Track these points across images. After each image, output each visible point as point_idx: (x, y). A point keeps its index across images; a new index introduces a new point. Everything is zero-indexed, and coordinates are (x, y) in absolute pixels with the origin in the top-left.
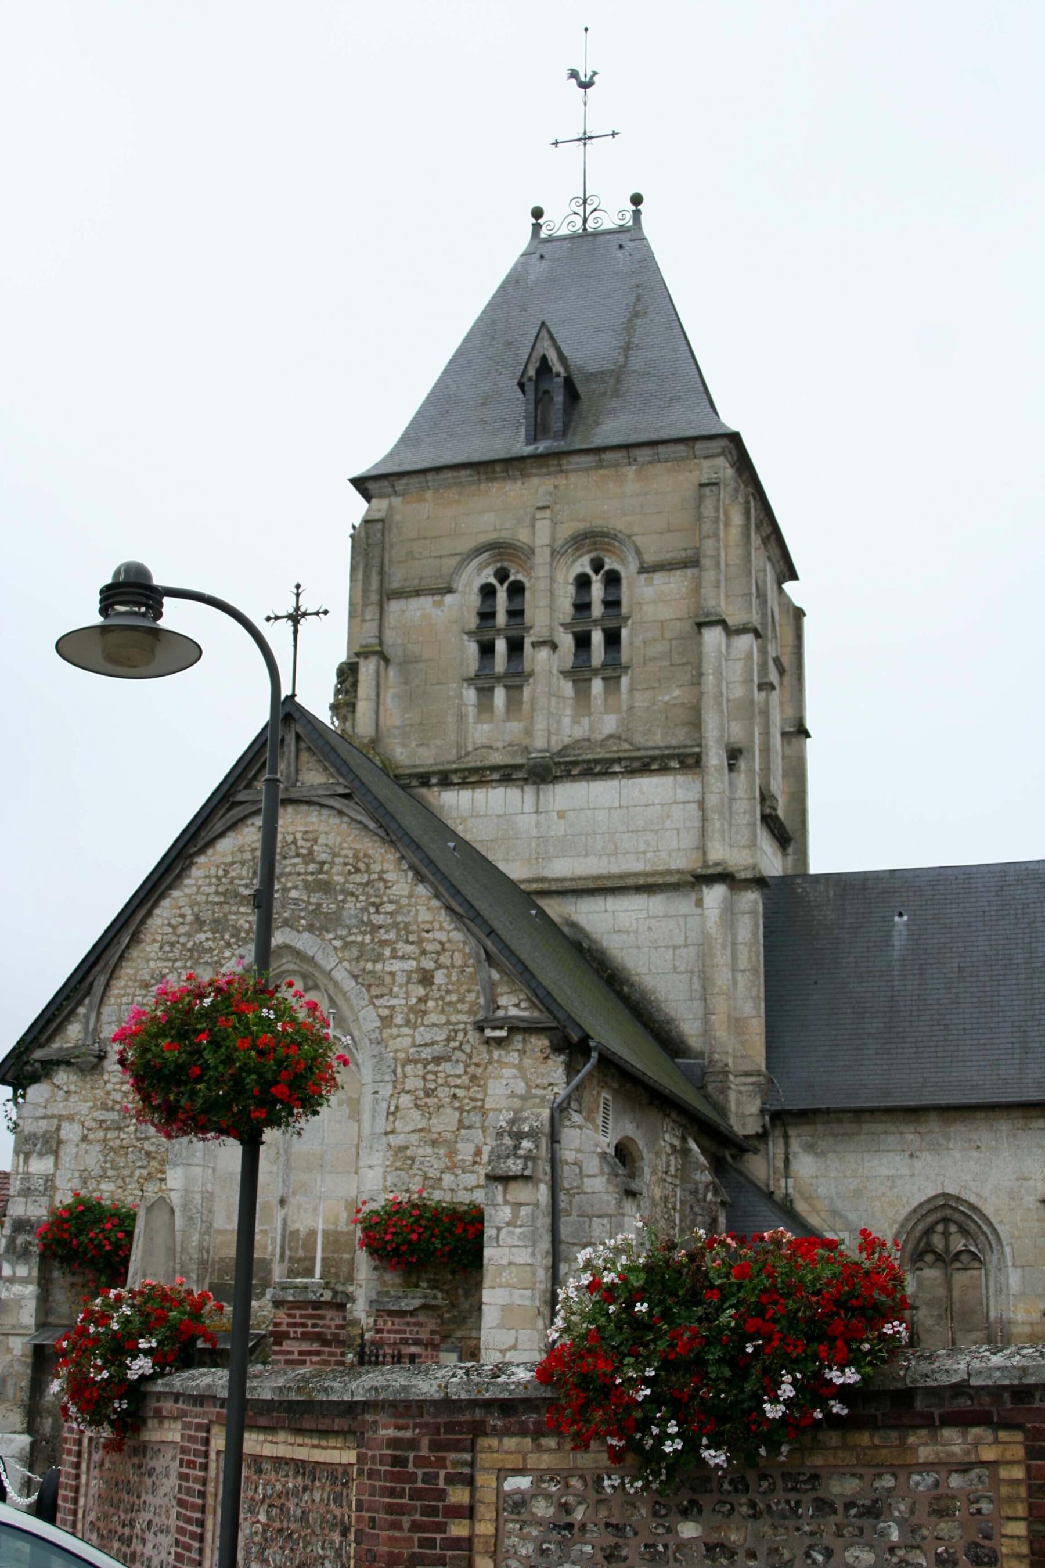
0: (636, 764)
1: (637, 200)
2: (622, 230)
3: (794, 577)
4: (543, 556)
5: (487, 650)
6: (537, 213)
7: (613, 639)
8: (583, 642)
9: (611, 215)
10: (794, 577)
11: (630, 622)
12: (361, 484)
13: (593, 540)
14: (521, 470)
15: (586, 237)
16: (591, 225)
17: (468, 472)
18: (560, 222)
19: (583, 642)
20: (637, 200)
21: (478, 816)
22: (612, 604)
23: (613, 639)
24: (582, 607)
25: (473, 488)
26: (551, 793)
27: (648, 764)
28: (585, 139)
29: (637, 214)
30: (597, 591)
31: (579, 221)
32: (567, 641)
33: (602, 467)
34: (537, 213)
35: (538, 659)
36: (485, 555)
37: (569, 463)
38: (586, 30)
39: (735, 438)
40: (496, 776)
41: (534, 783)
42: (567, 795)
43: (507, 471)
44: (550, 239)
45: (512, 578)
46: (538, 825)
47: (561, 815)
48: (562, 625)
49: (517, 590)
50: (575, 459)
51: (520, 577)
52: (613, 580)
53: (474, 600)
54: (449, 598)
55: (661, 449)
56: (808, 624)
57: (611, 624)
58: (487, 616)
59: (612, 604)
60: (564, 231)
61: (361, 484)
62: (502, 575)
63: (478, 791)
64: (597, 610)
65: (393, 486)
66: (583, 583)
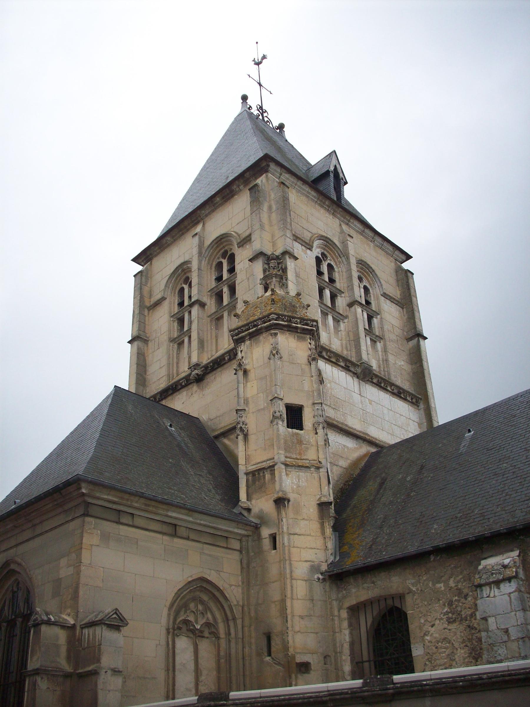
0: (395, 391)
6: (245, 98)
11: (378, 317)
14: (335, 211)
17: (315, 194)
21: (335, 383)
25: (313, 204)
26: (364, 387)
27: (400, 393)
33: (362, 235)
34: (245, 98)
37: (353, 223)
38: (257, 43)
40: (342, 364)
41: (358, 377)
42: (372, 392)
43: (329, 207)
45: (329, 262)
46: (362, 402)
47: (371, 402)
50: (356, 223)
51: (332, 263)
54: (308, 251)
55: (385, 244)
63: (334, 368)
65: (281, 174)
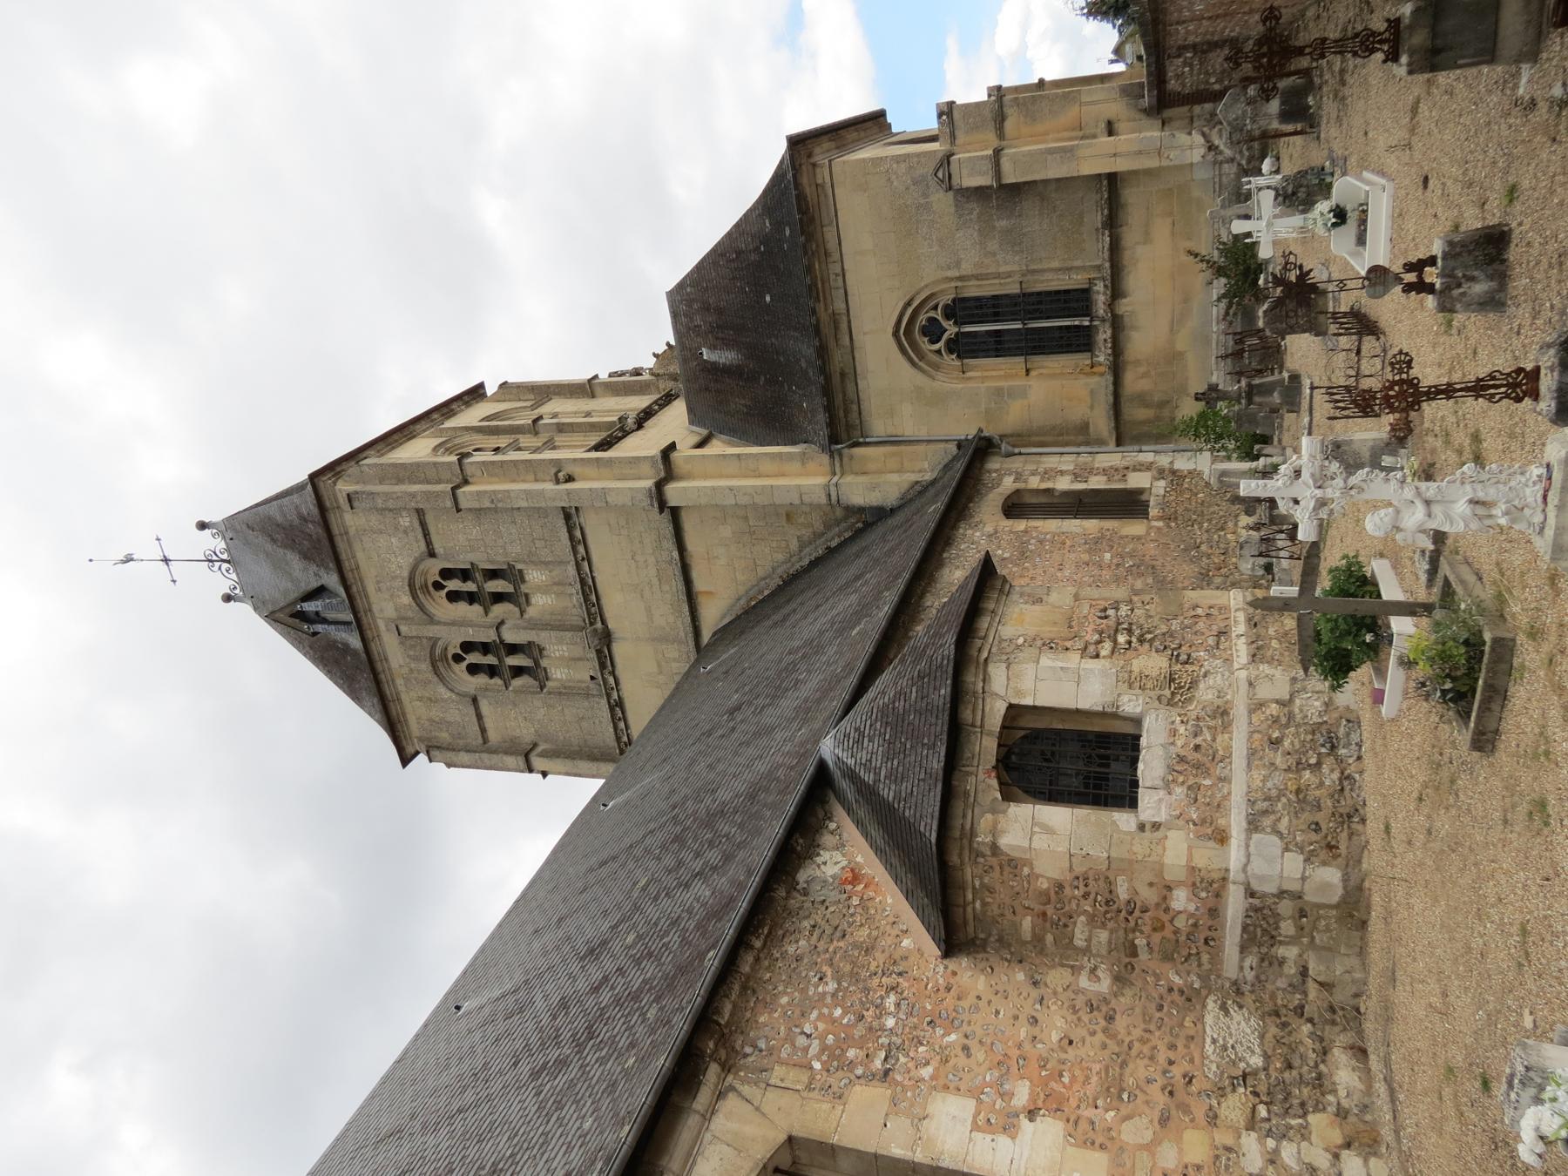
1: (202, 526)
3: (481, 386)
4: (433, 631)
7: (493, 574)
8: (498, 598)
10: (481, 386)
12: (405, 761)
16: (225, 557)
20: (202, 526)
22: (465, 575)
23: (493, 574)
24: (471, 598)
30: (454, 585)
31: (225, 566)
32: (499, 610)
34: (228, 598)
35: (510, 637)
36: (442, 670)
39: (314, 477)
48: (486, 613)
49: (468, 647)
52: (447, 574)
53: (482, 680)
56: (513, 379)
57: (478, 576)
59: (465, 575)
60: (234, 576)
61: (405, 761)
62: (458, 659)
66: (453, 597)
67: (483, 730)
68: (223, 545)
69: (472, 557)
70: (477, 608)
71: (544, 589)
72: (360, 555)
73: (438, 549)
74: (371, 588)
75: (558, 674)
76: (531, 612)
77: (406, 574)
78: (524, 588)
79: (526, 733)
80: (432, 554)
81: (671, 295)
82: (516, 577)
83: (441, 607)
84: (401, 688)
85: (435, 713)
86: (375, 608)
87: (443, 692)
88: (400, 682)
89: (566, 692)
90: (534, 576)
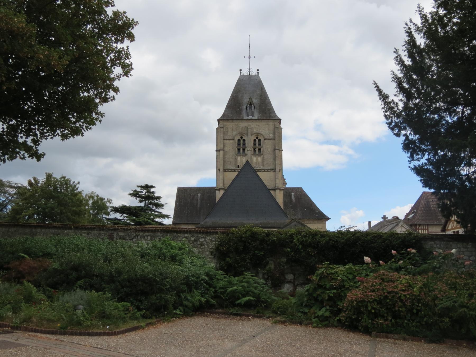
1: (258, 70)
2: (256, 76)
5: (239, 150)
6: (241, 70)
7: (260, 150)
9: (254, 73)
13: (258, 134)
15: (250, 76)
18: (245, 73)
19: (255, 150)
20: (258, 70)
22: (260, 144)
23: (260, 150)
24: (255, 144)
28: (250, 57)
29: (258, 73)
32: (253, 149)
34: (241, 70)
44: (243, 76)
52: (260, 140)
57: (260, 147)
58: (239, 144)
59: (260, 144)
64: (257, 145)
66: (255, 140)
67: (226, 140)
68: (253, 74)
69: (264, 147)
70: (253, 145)
71: (257, 160)
72: (264, 123)
73: (266, 141)
74: (257, 123)
75: (239, 158)
76: (253, 156)
77: (260, 132)
78: (257, 156)
79: (227, 149)
80: (265, 139)
81: (301, 188)
82: (260, 155)
83: (254, 137)
84: (235, 123)
85: (229, 130)
86: (253, 123)
87: (235, 133)
88: (237, 123)
89: (236, 160)
90: (260, 159)
